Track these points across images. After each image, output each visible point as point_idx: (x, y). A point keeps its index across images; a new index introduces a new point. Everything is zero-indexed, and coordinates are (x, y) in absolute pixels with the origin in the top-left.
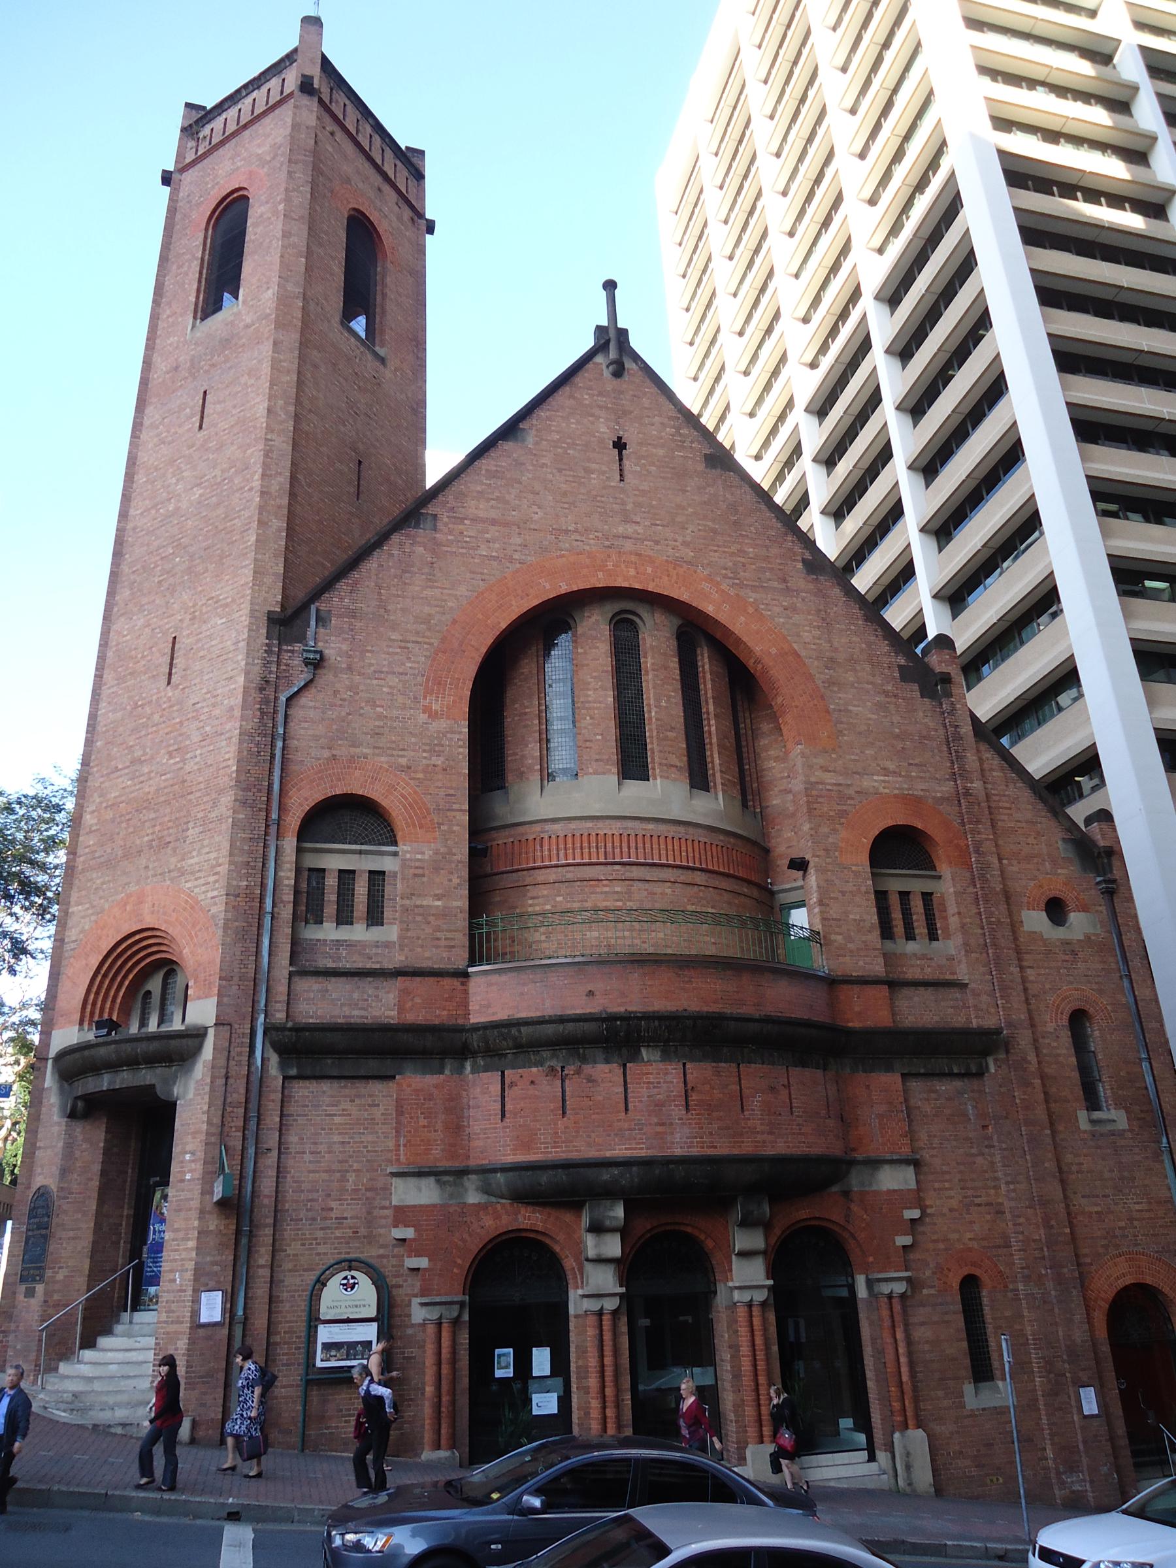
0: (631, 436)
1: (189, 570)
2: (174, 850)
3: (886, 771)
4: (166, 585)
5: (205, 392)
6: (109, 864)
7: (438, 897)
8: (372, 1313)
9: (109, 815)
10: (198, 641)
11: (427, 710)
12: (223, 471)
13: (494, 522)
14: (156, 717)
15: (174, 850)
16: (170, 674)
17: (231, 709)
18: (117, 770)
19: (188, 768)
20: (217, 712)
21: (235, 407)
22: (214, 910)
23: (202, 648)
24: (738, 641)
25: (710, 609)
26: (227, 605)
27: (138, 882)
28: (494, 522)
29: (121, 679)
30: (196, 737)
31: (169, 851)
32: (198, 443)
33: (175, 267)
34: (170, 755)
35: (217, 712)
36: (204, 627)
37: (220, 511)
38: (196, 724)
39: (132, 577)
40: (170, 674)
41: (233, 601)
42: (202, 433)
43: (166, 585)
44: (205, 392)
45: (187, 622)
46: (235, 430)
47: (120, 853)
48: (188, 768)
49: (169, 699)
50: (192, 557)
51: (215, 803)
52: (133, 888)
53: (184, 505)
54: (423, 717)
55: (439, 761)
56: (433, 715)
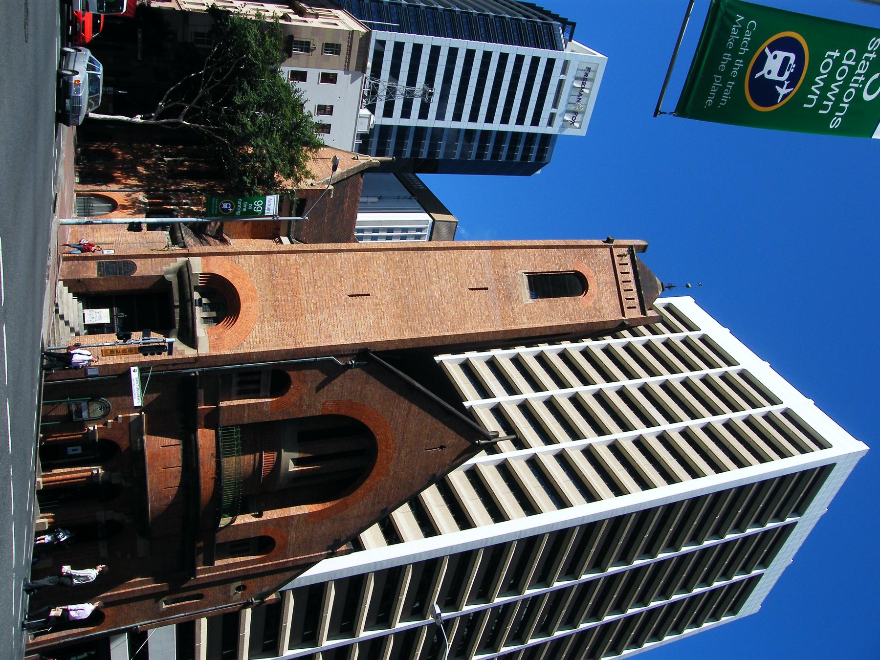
0: (446, 450)
1: (400, 297)
3: (297, 538)
4: (396, 284)
7: (248, 415)
8: (91, 416)
11: (326, 402)
12: (444, 309)
13: (408, 413)
14: (334, 291)
16: (352, 296)
17: (330, 337)
18: (313, 271)
19: (308, 316)
20: (330, 328)
22: (245, 343)
24: (354, 490)
25: (367, 482)
26: (378, 324)
27: (261, 296)
28: (408, 413)
29: (356, 264)
30: (320, 318)
33: (560, 254)
34: (316, 304)
35: (330, 328)
37: (425, 311)
40: (352, 296)
41: (380, 328)
42: (466, 290)
43: (396, 283)
46: (462, 313)
47: (275, 282)
48: (308, 316)
49: (341, 298)
50: (406, 297)
51: (290, 335)
52: (259, 293)
54: (323, 401)
55: (305, 408)
56: (324, 404)
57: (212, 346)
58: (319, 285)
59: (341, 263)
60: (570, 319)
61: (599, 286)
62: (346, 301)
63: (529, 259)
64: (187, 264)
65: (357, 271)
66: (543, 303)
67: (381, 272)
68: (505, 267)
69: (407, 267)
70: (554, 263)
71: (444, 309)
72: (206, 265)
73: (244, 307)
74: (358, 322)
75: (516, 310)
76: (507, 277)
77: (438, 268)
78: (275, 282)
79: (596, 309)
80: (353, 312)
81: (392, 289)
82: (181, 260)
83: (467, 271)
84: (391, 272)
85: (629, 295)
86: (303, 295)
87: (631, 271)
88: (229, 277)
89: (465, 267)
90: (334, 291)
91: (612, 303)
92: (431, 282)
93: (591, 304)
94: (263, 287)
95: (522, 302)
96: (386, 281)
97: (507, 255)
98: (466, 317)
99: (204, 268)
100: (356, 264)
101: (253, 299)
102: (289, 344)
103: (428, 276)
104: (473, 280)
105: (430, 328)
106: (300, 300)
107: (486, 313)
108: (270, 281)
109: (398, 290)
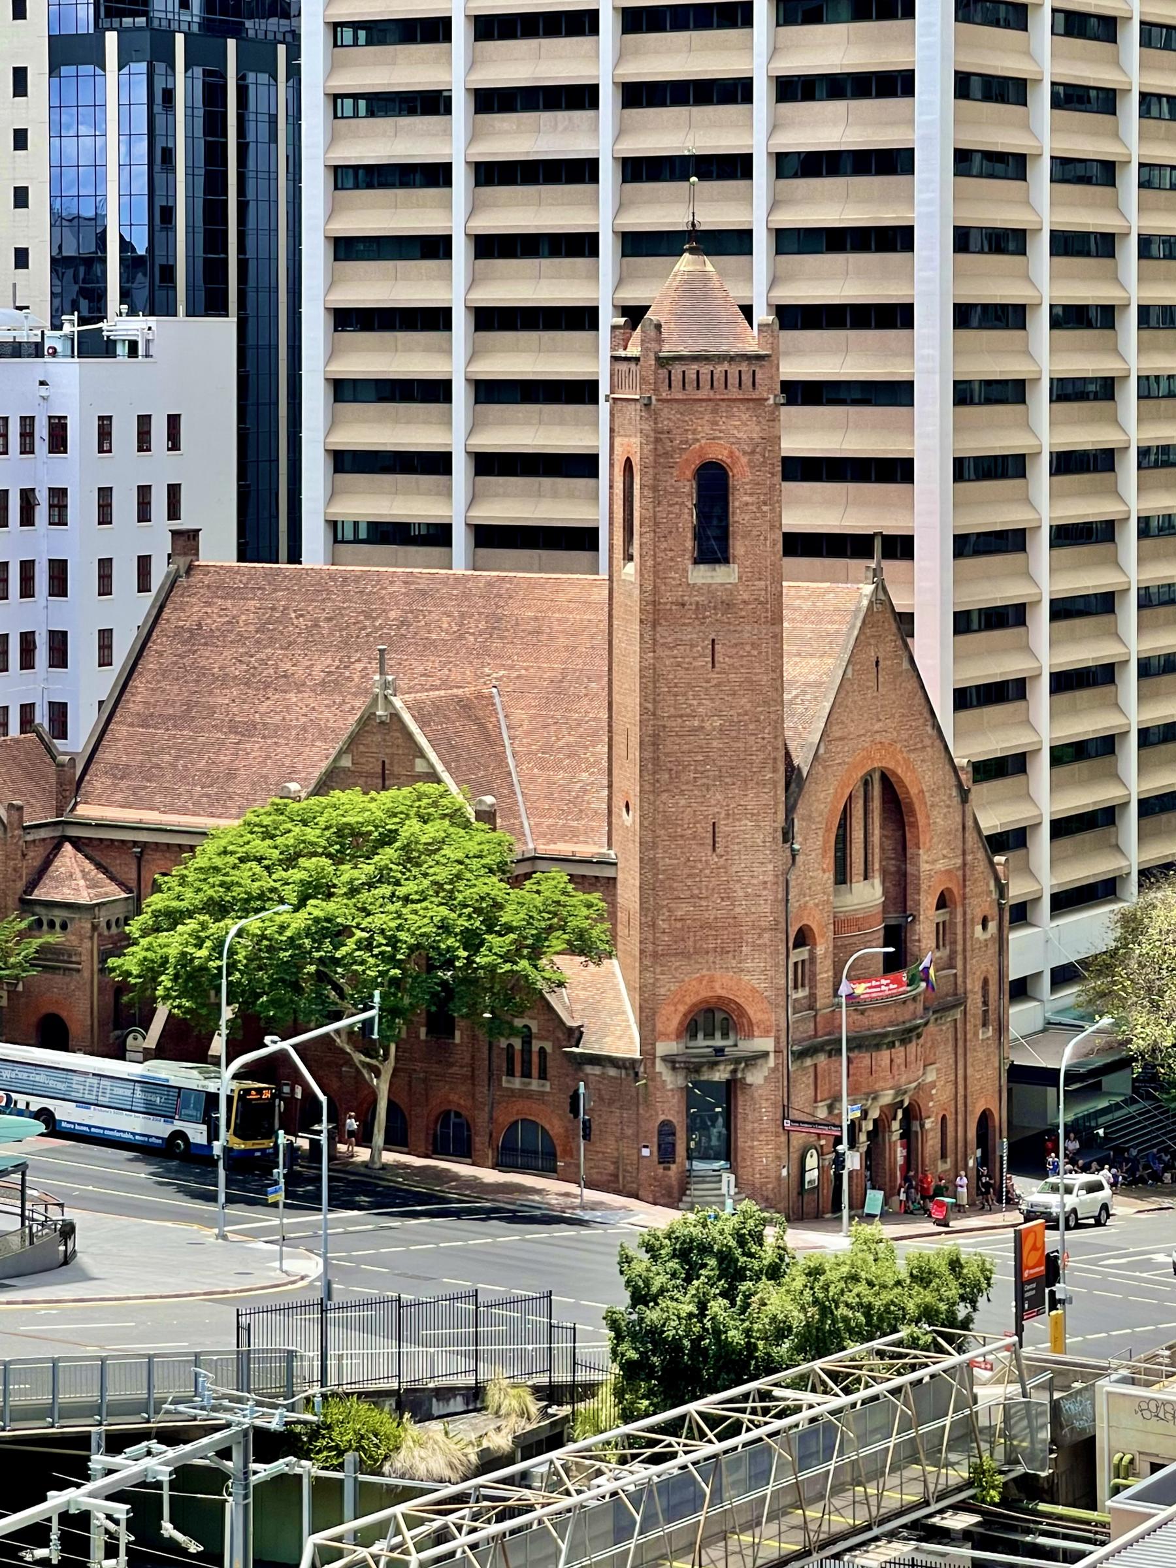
2: (734, 957)
5: (713, 641)
6: (685, 955)
9: (679, 925)
10: (734, 831)
14: (707, 872)
15: (734, 957)
17: (765, 883)
19: (738, 910)
20: (755, 881)
21: (742, 666)
23: (737, 837)
26: (753, 815)
27: (709, 969)
31: (730, 955)
32: (714, 682)
34: (722, 899)
35: (755, 881)
36: (737, 824)
38: (738, 886)
39: (669, 765)
41: (758, 814)
44: (713, 641)
45: (723, 815)
47: (692, 950)
48: (738, 910)
49: (716, 863)
51: (760, 936)
52: (704, 972)
53: (707, 725)
56: (824, 871)
57: (766, 1033)
58: (696, 892)
59: (670, 858)
60: (765, 504)
61: (720, 438)
62: (722, 856)
63: (672, 559)
64: (665, 1059)
65: (682, 836)
66: (738, 547)
67: (683, 802)
68: (683, 605)
69: (679, 763)
70: (679, 516)
71: (739, 714)
72: (665, 1036)
73: (721, 992)
74: (749, 844)
75: (746, 597)
76: (697, 603)
77: (681, 716)
78: (692, 950)
79: (753, 452)
80: (736, 847)
81: (708, 790)
82: (660, 1066)
83: (687, 669)
84: (684, 788)
85: (733, 380)
86: (711, 915)
87: (695, 367)
88: (682, 1009)
89: (682, 673)
90: (707, 872)
91: (744, 417)
92: (703, 727)
93: (744, 460)
94: (699, 966)
95: (735, 585)
96: (696, 797)
97: (668, 597)
98: (751, 682)
99: (672, 1040)
100: (672, 838)
101: (712, 980)
102: (772, 940)
103: (694, 731)
104: (699, 663)
105: (763, 738)
106: (716, 918)
107: (748, 648)
108: (689, 958)
109: (711, 782)
